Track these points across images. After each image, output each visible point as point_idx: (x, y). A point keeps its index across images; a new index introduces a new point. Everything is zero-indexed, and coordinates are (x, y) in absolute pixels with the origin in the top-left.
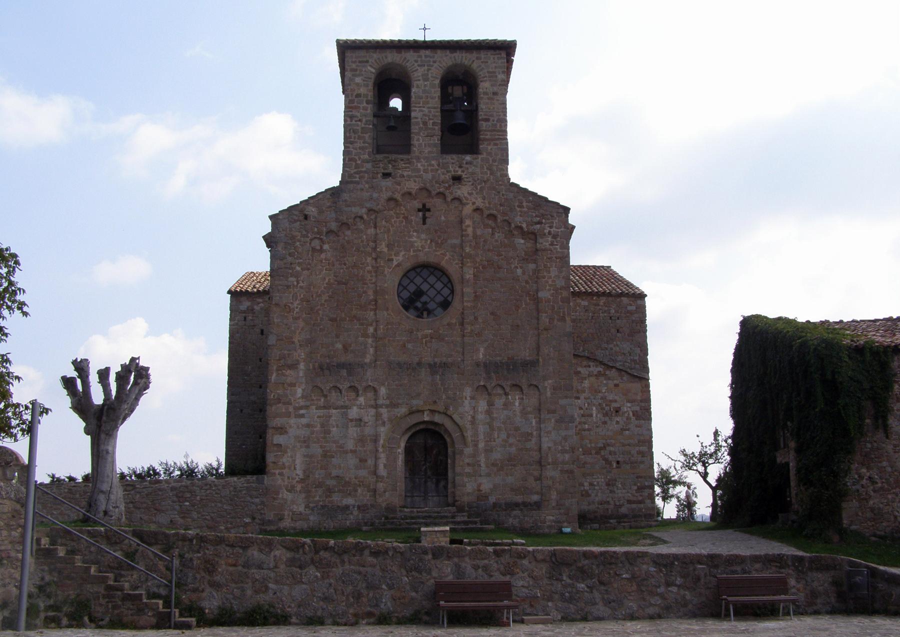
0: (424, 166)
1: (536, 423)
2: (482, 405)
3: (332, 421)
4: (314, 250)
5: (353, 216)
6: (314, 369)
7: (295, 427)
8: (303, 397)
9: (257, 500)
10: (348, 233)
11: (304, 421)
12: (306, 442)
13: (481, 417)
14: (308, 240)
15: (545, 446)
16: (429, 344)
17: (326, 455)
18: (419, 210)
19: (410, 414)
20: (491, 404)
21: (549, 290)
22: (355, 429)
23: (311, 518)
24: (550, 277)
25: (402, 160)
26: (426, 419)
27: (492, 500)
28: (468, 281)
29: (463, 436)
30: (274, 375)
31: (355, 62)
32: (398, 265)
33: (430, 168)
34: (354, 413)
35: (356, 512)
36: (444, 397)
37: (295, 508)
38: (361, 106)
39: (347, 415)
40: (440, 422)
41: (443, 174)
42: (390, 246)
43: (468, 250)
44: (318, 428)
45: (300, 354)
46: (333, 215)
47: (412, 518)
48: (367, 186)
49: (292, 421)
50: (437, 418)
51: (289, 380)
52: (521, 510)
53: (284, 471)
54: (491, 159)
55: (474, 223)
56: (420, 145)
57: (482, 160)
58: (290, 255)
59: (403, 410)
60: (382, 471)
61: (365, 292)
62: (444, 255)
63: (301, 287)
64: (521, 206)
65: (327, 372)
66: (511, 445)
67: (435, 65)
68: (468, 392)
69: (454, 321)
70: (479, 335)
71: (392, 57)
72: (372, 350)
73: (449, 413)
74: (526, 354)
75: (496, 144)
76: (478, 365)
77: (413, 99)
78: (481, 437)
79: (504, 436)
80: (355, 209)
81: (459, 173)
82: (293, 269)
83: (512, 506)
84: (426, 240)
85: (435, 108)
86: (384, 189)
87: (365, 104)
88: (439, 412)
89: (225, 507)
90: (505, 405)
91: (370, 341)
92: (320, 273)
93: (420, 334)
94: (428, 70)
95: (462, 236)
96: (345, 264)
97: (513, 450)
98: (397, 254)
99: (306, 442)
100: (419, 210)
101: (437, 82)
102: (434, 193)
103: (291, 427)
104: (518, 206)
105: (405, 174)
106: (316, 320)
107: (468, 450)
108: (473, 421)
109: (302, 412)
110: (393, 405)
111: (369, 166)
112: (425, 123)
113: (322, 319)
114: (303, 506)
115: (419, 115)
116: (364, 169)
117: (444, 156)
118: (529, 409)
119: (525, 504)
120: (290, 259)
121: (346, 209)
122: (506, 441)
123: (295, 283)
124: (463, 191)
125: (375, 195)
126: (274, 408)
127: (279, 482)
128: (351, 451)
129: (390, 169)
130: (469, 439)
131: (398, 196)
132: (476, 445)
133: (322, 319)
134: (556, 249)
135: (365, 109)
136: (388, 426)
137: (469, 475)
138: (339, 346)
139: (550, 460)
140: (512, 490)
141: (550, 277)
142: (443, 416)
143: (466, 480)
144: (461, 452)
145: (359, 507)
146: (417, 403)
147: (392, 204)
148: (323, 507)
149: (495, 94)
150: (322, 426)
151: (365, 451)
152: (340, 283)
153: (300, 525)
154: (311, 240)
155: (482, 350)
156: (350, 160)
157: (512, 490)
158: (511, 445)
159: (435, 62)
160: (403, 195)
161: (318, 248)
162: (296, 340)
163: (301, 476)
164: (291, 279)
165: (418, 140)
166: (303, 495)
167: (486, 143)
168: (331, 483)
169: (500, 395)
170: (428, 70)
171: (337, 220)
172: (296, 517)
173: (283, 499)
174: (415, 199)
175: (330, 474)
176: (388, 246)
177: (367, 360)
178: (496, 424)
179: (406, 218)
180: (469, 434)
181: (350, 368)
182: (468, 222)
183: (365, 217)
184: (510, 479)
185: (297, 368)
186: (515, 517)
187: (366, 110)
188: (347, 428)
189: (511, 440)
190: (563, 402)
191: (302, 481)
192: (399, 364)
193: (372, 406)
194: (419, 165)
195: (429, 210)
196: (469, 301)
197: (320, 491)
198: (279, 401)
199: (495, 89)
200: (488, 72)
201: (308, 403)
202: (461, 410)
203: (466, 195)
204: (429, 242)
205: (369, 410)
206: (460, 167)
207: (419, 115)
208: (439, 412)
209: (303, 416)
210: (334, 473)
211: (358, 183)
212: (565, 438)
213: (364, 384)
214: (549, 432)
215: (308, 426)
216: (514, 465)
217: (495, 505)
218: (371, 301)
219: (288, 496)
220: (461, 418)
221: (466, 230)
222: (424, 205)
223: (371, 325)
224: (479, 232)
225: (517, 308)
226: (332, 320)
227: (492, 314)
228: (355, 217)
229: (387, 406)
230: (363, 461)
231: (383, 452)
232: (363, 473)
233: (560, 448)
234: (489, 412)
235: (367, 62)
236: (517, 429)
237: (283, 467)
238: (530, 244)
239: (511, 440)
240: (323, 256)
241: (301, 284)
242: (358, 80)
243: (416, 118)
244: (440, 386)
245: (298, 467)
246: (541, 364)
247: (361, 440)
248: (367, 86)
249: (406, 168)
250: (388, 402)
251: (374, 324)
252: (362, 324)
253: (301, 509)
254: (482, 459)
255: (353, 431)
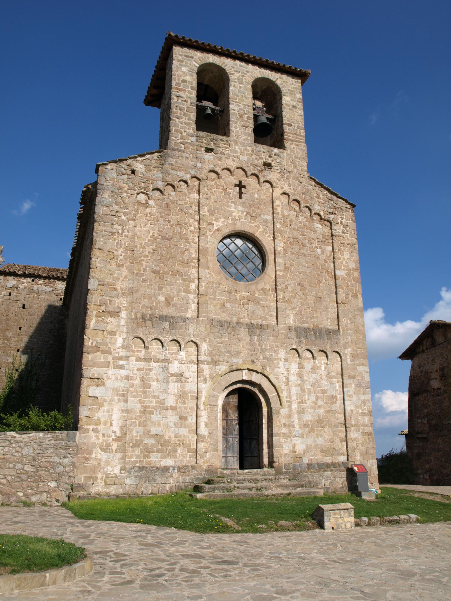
0: (240, 149)
1: (339, 386)
2: (294, 368)
3: (153, 374)
4: (139, 202)
5: (178, 179)
6: (136, 318)
7: (113, 378)
8: (123, 347)
9: (66, 460)
10: (173, 193)
11: (123, 373)
12: (124, 396)
13: (293, 378)
14: (135, 193)
15: (348, 409)
16: (246, 306)
17: (145, 411)
18: (236, 185)
19: (230, 372)
20: (301, 367)
21: (344, 270)
22: (176, 384)
23: (128, 481)
24: (344, 259)
25: (222, 140)
26: (245, 378)
27: (306, 461)
28: (279, 252)
29: (279, 396)
30: (93, 321)
31: (181, 55)
32: (218, 230)
33: (246, 152)
34: (175, 367)
35: (176, 475)
36: (261, 357)
37: (109, 470)
38: (187, 90)
39: (167, 369)
40: (258, 382)
41: (256, 159)
42: (212, 212)
43: (278, 225)
44: (137, 381)
45: (123, 302)
46: (160, 175)
47: (239, 482)
48: (191, 155)
49: (111, 372)
50: (255, 378)
51: (109, 328)
52: (332, 471)
53: (99, 427)
54: (294, 156)
55: (282, 203)
56: (237, 132)
57: (287, 154)
58: (116, 203)
59: (224, 368)
60: (203, 430)
61: (187, 250)
62: (258, 227)
63: (126, 236)
64: (318, 197)
65: (149, 323)
66: (319, 407)
67: (248, 74)
68: (282, 354)
69: (267, 287)
70: (289, 302)
71: (211, 58)
72: (194, 306)
73: (266, 374)
74: (328, 323)
75: (297, 145)
76: (290, 329)
77: (231, 95)
78: (294, 398)
79: (313, 398)
80: (181, 174)
81: (269, 161)
82: (118, 217)
83: (324, 467)
84: (243, 212)
85: (248, 106)
86: (207, 161)
87: (190, 89)
88: (257, 372)
89: (26, 468)
90: (313, 368)
91: (192, 296)
92: (144, 227)
93: (238, 296)
94: (243, 76)
95: (273, 213)
96: (169, 221)
97: (321, 412)
98: (217, 220)
99: (124, 396)
100: (236, 185)
101: (250, 87)
102: (249, 173)
103: (108, 378)
104: (317, 197)
105: (225, 152)
106: (140, 270)
107: (284, 411)
108: (287, 384)
109: (121, 362)
110: (214, 362)
111: (194, 139)
112: (241, 116)
113: (145, 270)
114: (119, 467)
115: (237, 108)
116: (189, 141)
117: (257, 145)
118: (333, 374)
119: (334, 465)
120: (116, 208)
121: (172, 172)
122: (316, 403)
123: (120, 231)
124: (272, 176)
125: (199, 165)
126: (90, 356)
127: (94, 439)
128: (174, 408)
129: (212, 146)
130: (284, 400)
131: (218, 169)
132: (290, 407)
133: (145, 270)
134: (347, 236)
135: (189, 92)
136: (209, 383)
137: (285, 436)
138: (161, 298)
139: (353, 423)
140: (322, 451)
141: (344, 259)
142: (260, 375)
143: (283, 440)
144: (279, 412)
145: (179, 469)
146: (237, 362)
147: (213, 175)
148: (141, 468)
149: (294, 107)
150: (142, 379)
151: (185, 408)
152: (164, 238)
153: (113, 490)
154: (138, 194)
155: (292, 317)
156: (176, 131)
157: (322, 451)
158: (319, 407)
159: (248, 72)
160: (223, 170)
161: (144, 202)
162: (119, 288)
163: (118, 434)
164: (116, 226)
165: (236, 127)
166: (120, 455)
167: (289, 142)
168: (150, 442)
169: (308, 358)
170: (243, 76)
171: (163, 180)
172: (110, 480)
173: (96, 459)
174: (233, 176)
175: (149, 432)
176: (208, 211)
177: (189, 315)
178: (307, 386)
179: (225, 190)
180: (284, 395)
181: (172, 321)
182: (277, 203)
183: (189, 182)
184: (320, 441)
185: (119, 316)
186: (327, 478)
187: (191, 94)
188: (168, 382)
189: (320, 402)
190: (360, 369)
191: (118, 439)
192: (221, 323)
193: (193, 362)
194: (237, 147)
195: (244, 187)
196: (280, 271)
197: (137, 452)
198: (97, 349)
199: (295, 104)
200: (289, 90)
201: (128, 354)
202: (276, 370)
203: (275, 180)
204: (245, 213)
205: (191, 365)
206: (270, 157)
207: (237, 108)
208: (257, 372)
209: (122, 367)
210: (154, 430)
211: (183, 152)
212: (364, 402)
213: (187, 339)
214: (350, 396)
215: (127, 378)
216: (323, 427)
217: (309, 465)
218: (194, 259)
219: (103, 456)
220: (277, 379)
221: (276, 209)
222: (240, 182)
223: (193, 281)
224: (286, 213)
225: (319, 282)
226: (154, 272)
227: (299, 284)
228: (180, 181)
229: (208, 363)
230: (183, 418)
231: (205, 409)
232: (183, 431)
233: (360, 411)
234: (300, 375)
235: (192, 57)
236: (324, 392)
237: (98, 423)
238: (327, 230)
239: (320, 402)
240: (148, 210)
241: (126, 233)
242: (184, 69)
243: (234, 110)
244: (257, 347)
245: (114, 423)
246: (341, 333)
247: (182, 397)
248: (192, 76)
249: (226, 148)
250: (209, 359)
251: (196, 281)
252: (184, 280)
253: (117, 471)
254: (295, 418)
255: (174, 387)
